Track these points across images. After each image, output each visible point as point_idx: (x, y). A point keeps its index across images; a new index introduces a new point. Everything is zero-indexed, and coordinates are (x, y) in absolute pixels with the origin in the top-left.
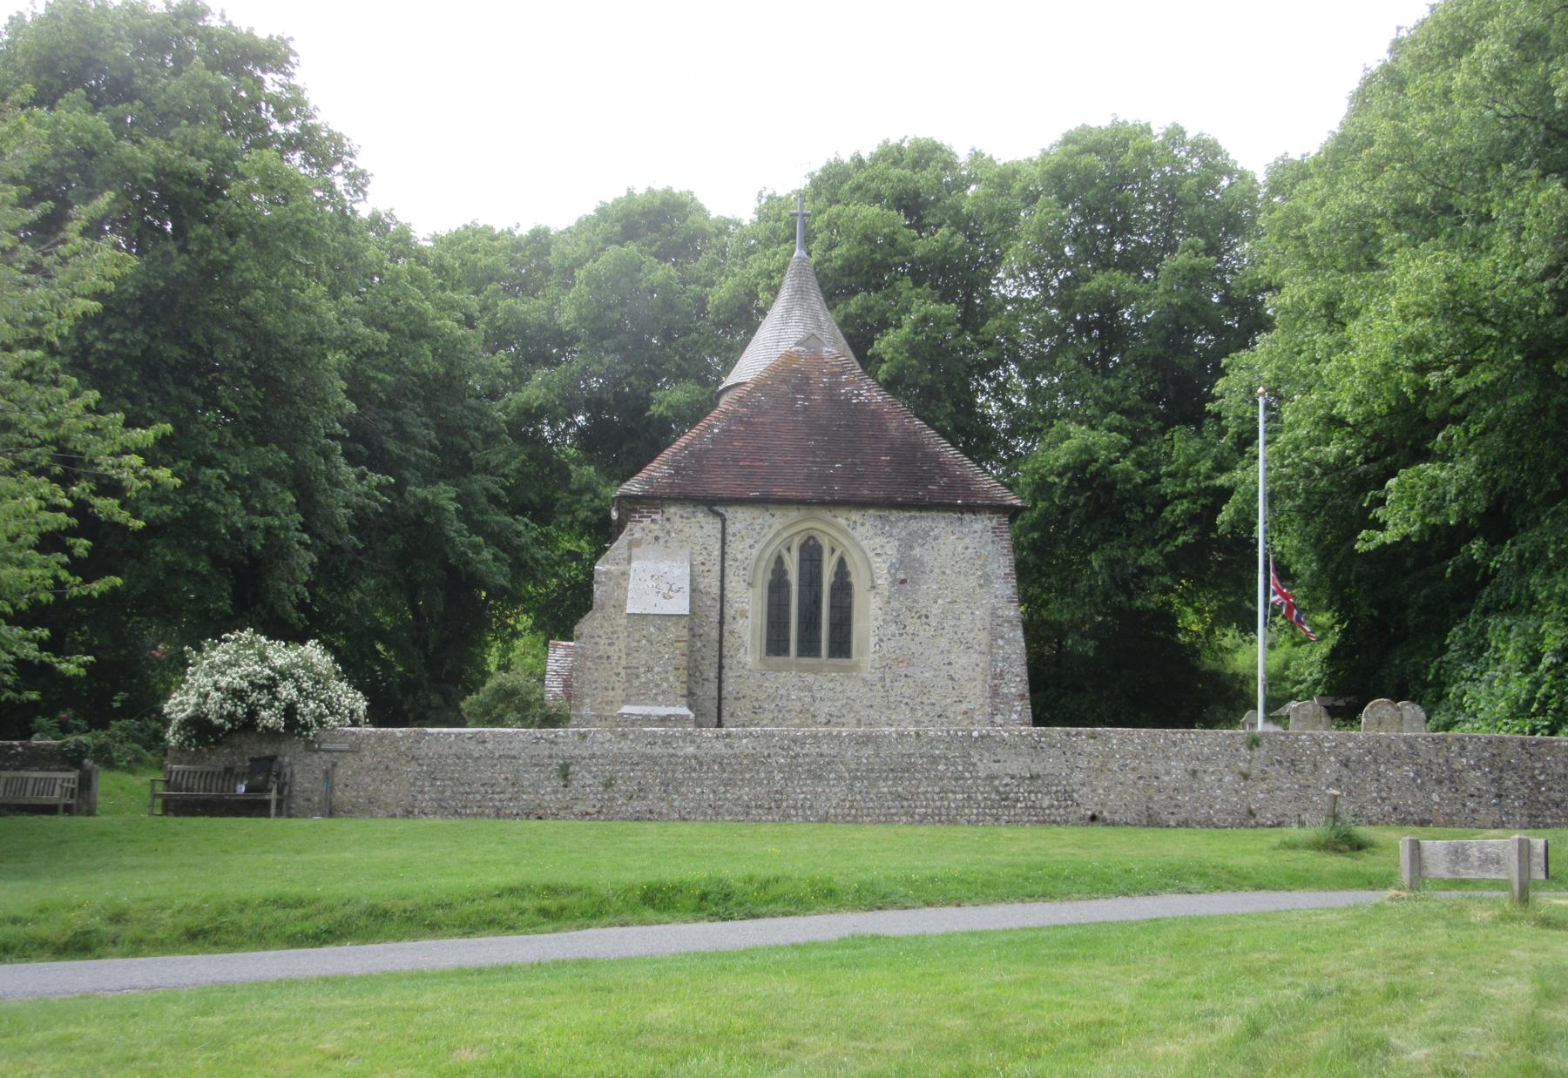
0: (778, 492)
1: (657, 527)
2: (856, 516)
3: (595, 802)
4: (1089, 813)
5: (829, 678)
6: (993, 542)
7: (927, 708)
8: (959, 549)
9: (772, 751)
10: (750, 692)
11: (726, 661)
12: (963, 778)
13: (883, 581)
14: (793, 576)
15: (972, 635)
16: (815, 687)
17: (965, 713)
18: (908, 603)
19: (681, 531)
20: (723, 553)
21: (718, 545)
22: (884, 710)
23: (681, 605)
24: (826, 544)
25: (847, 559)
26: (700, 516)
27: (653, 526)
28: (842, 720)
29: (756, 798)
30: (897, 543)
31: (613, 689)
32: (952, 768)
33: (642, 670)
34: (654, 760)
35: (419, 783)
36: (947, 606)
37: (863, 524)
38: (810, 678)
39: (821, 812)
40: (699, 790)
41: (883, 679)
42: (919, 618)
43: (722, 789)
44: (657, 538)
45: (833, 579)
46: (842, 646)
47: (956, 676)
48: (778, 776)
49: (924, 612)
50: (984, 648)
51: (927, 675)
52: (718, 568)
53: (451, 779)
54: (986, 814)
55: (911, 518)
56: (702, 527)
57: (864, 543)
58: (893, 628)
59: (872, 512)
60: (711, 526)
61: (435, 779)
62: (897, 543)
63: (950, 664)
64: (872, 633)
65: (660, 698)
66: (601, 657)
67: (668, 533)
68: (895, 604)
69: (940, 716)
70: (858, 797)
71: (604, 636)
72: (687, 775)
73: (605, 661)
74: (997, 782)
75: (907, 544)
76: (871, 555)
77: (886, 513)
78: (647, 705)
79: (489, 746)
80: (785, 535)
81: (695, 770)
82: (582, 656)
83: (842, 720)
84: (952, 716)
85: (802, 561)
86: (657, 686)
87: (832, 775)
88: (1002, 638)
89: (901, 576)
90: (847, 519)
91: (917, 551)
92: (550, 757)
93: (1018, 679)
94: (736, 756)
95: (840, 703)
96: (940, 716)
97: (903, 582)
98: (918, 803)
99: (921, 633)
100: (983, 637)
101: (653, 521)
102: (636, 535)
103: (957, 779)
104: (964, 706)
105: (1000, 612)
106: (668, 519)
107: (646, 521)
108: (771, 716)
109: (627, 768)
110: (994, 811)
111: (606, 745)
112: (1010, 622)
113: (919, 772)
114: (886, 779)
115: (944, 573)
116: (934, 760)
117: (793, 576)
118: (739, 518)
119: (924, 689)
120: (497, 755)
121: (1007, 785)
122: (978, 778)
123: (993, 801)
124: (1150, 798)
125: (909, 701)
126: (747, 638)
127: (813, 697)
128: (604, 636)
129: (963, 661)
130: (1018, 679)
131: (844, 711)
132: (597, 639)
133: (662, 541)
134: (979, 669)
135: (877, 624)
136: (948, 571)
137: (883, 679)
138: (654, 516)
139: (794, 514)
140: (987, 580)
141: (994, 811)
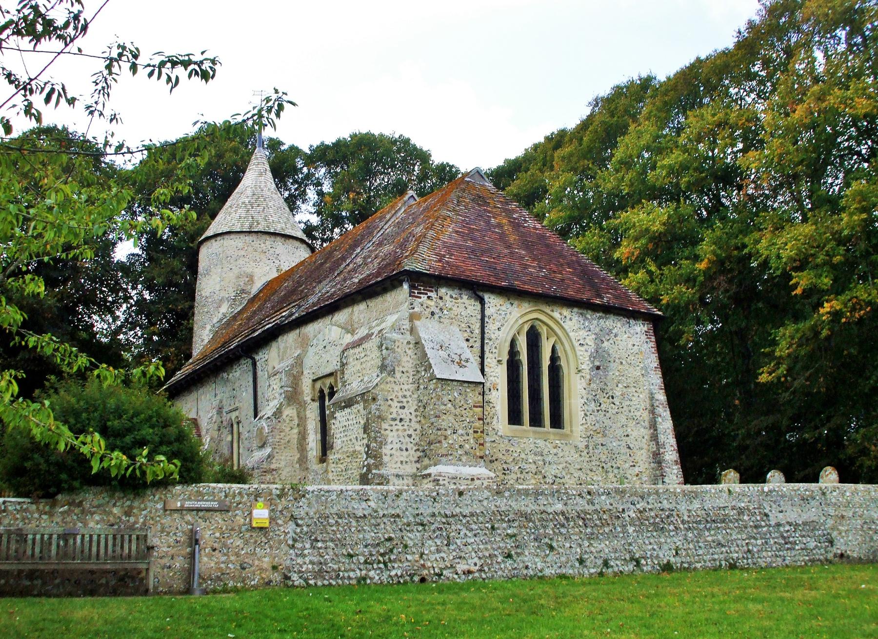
2: (566, 312)
3: (476, 560)
4: (839, 552)
5: (554, 445)
8: (630, 346)
9: (625, 506)
10: (501, 456)
12: (761, 527)
13: (586, 366)
14: (524, 357)
15: (638, 414)
16: (545, 452)
17: (637, 475)
18: (602, 385)
19: (451, 309)
20: (483, 333)
21: (478, 325)
22: (589, 472)
24: (543, 331)
25: (558, 347)
26: (465, 297)
27: (429, 302)
31: (407, 450)
32: (753, 518)
33: (449, 432)
34: (527, 517)
35: (299, 545)
36: (625, 390)
37: (571, 319)
38: (541, 443)
40: (568, 545)
43: (586, 544)
44: (433, 314)
46: (557, 421)
47: (631, 446)
48: (631, 529)
49: (610, 394)
50: (647, 424)
51: (614, 444)
54: (777, 556)
55: (600, 318)
57: (571, 334)
59: (576, 310)
60: (473, 307)
61: (316, 540)
62: (594, 336)
63: (628, 436)
66: (394, 420)
67: (441, 309)
68: (594, 386)
72: (557, 531)
73: (398, 422)
74: (782, 529)
75: (599, 340)
76: (576, 344)
77: (585, 312)
79: (372, 504)
80: (521, 322)
81: (563, 526)
82: (379, 417)
84: (629, 477)
86: (461, 446)
87: (672, 527)
89: (597, 363)
90: (561, 314)
91: (606, 344)
92: (434, 515)
94: (596, 511)
95: (560, 467)
97: (598, 368)
99: (610, 410)
100: (646, 415)
101: (429, 297)
102: (416, 309)
103: (756, 527)
104: (636, 470)
106: (441, 298)
107: (424, 298)
108: (515, 478)
109: (505, 525)
110: (781, 553)
111: (485, 503)
113: (731, 522)
114: (709, 530)
115: (621, 363)
116: (741, 512)
117: (524, 357)
119: (613, 455)
120: (381, 514)
121: (788, 531)
122: (770, 526)
123: (779, 544)
124: (871, 539)
125: (604, 465)
126: (498, 408)
127: (544, 460)
128: (395, 400)
131: (564, 473)
132: (390, 402)
133: (436, 316)
134: (644, 440)
135: (583, 401)
136: (624, 362)
137: (587, 447)
138: (430, 294)
139: (526, 307)
141: (781, 553)
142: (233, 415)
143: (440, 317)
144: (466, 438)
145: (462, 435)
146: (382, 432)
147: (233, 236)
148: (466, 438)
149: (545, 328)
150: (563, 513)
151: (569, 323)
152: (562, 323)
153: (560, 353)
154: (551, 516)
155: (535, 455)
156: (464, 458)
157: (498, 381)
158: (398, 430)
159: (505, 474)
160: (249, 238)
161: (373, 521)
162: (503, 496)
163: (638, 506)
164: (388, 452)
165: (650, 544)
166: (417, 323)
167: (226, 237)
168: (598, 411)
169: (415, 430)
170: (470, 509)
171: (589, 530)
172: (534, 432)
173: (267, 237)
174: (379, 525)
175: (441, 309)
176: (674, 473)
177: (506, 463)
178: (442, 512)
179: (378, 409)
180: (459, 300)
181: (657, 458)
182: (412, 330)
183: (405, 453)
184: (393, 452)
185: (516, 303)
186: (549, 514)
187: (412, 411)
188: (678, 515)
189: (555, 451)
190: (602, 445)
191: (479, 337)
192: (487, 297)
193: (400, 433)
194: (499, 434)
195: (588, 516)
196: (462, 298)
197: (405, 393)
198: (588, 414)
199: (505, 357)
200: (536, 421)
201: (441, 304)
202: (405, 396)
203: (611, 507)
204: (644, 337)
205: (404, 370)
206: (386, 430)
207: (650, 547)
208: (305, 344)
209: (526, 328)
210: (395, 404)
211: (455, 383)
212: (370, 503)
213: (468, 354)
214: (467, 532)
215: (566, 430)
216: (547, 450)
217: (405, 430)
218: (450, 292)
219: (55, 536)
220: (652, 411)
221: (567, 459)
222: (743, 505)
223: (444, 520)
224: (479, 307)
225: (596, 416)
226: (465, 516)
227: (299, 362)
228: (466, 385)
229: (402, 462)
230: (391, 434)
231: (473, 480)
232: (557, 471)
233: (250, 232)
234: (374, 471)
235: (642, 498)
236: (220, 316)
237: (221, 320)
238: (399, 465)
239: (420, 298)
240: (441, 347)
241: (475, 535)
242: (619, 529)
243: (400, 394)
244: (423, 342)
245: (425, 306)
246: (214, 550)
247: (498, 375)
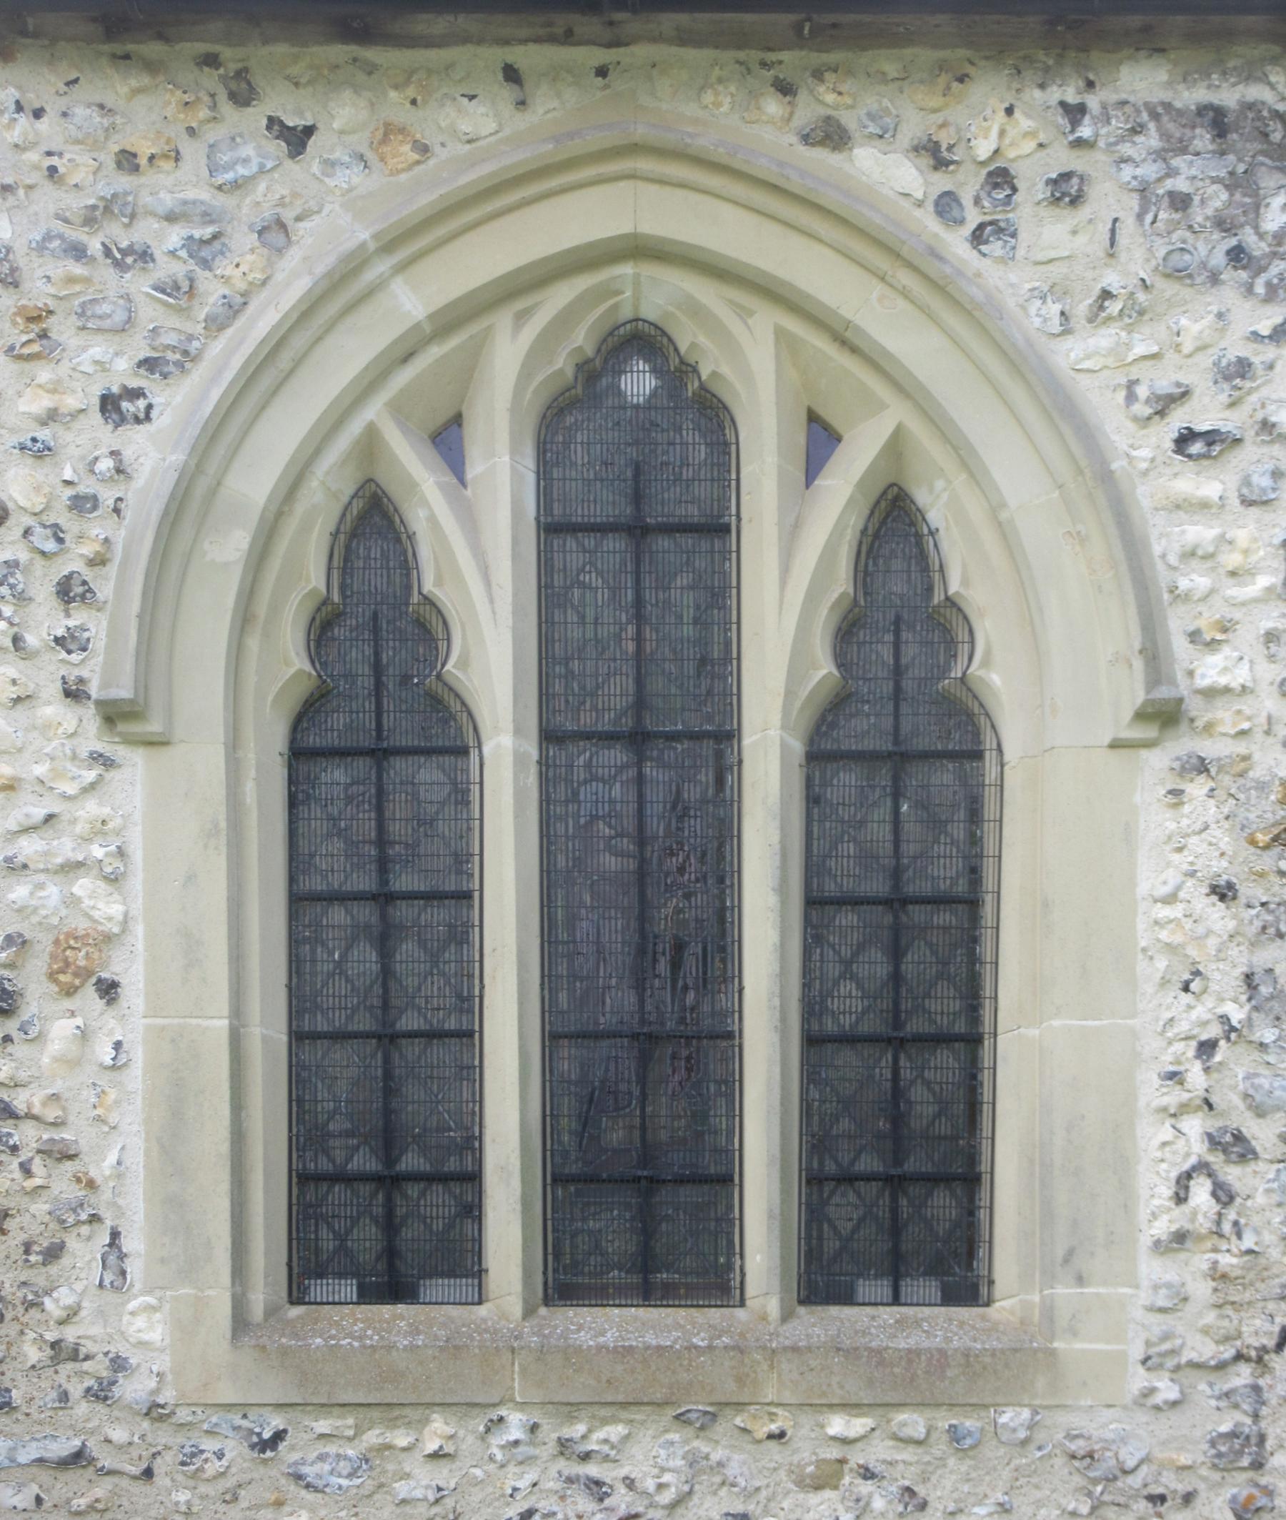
45: (824, 668)
64: (1152, 1093)
152: (956, 243)
157: (108, 909)
194: (134, 1389)
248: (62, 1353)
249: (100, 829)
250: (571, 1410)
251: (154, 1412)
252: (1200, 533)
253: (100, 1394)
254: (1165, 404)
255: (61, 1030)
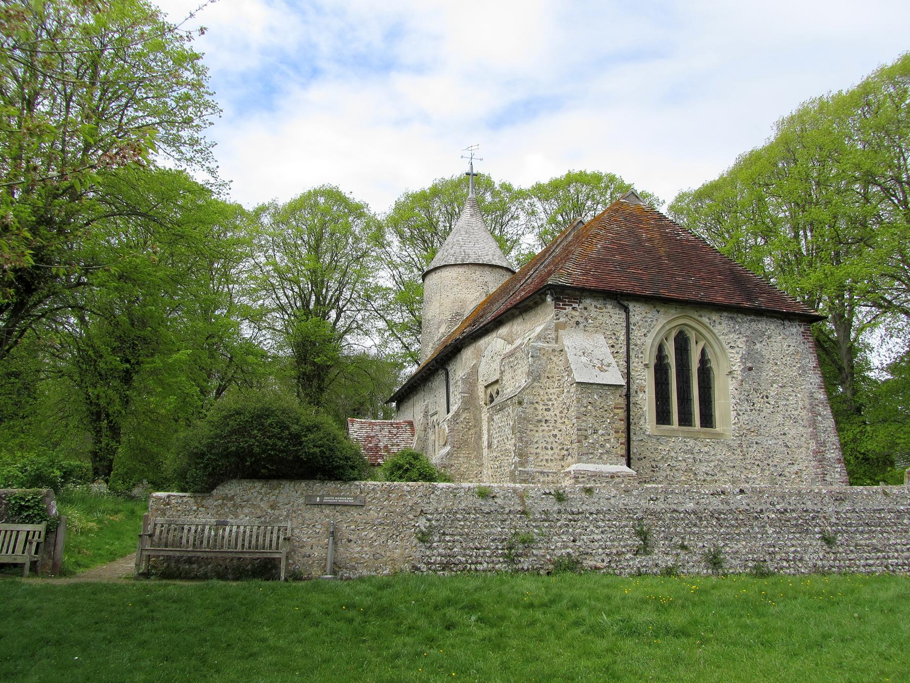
0: (664, 293)
1: (577, 314)
2: (715, 317)
6: (804, 343)
7: (772, 469)
9: (764, 507)
10: (649, 454)
11: (622, 425)
13: (737, 368)
14: (672, 361)
15: (796, 413)
19: (596, 318)
20: (628, 339)
21: (624, 332)
22: (743, 470)
23: (615, 377)
24: (692, 336)
26: (610, 307)
27: (574, 313)
28: (715, 478)
29: (751, 552)
30: (745, 339)
31: (552, 449)
33: (590, 432)
36: (780, 390)
37: (720, 323)
38: (691, 443)
39: (810, 564)
40: (701, 544)
41: (740, 445)
42: (762, 398)
46: (707, 420)
47: (789, 444)
49: (765, 393)
51: (770, 443)
52: (624, 349)
53: (461, 535)
55: (752, 321)
56: (612, 316)
57: (720, 338)
58: (746, 406)
59: (725, 314)
61: (444, 534)
62: (745, 339)
63: (784, 434)
65: (605, 457)
66: (540, 421)
67: (586, 319)
69: (780, 475)
70: (841, 550)
71: (541, 403)
75: (751, 342)
77: (735, 316)
78: (595, 463)
79: (499, 501)
80: (668, 328)
81: (695, 525)
83: (715, 478)
84: (788, 475)
85: (676, 349)
86: (602, 446)
87: (817, 529)
88: (820, 415)
91: (758, 346)
92: (559, 512)
93: (835, 447)
94: (731, 511)
95: (712, 464)
96: (780, 475)
97: (750, 369)
98: (891, 554)
101: (573, 308)
102: (561, 320)
104: (795, 468)
105: (815, 396)
106: (586, 309)
107: (569, 309)
108: (665, 475)
111: (612, 501)
112: (822, 403)
115: (776, 364)
117: (672, 361)
118: (638, 312)
119: (769, 454)
120: (507, 510)
128: (541, 403)
129: (793, 432)
130: (835, 447)
133: (581, 326)
137: (740, 445)
139: (673, 313)
140: (803, 371)
142: (435, 418)
143: (585, 326)
144: (606, 437)
145: (603, 435)
146: (528, 432)
147: (448, 269)
148: (606, 437)
149: (693, 333)
150: (694, 513)
151: (719, 327)
152: (711, 327)
153: (710, 355)
154: (682, 515)
155: (685, 453)
156: (605, 457)
158: (543, 431)
159: (654, 471)
160: (461, 270)
161: (500, 517)
162: (631, 495)
163: (778, 507)
164: (533, 451)
165: (793, 546)
166: (561, 332)
167: (443, 270)
168: (751, 410)
169: (560, 431)
170: (597, 507)
171: (723, 530)
172: (683, 431)
173: (477, 268)
174: (505, 520)
175: (586, 319)
176: (838, 473)
177: (654, 460)
178: (569, 509)
179: (524, 412)
180: (604, 310)
181: (819, 456)
182: (557, 340)
183: (550, 452)
184: (539, 451)
185: (662, 310)
186: (680, 513)
187: (557, 412)
188: (824, 517)
189: (706, 449)
190: (757, 443)
191: (625, 343)
192: (631, 306)
193: (546, 434)
195: (722, 516)
196: (606, 308)
197: (550, 397)
198: (741, 413)
199: (653, 362)
200: (685, 419)
201: (586, 314)
202: (550, 400)
203: (748, 508)
204: (800, 338)
205: (550, 375)
206: (531, 430)
207: (793, 549)
208: (479, 355)
209: (674, 334)
210: (540, 407)
211: (595, 387)
212: (496, 500)
213: (610, 359)
214: (594, 529)
215: (719, 428)
216: (697, 448)
217: (550, 431)
218: (594, 303)
219: (207, 527)
220: (812, 410)
221: (719, 457)
222: (902, 508)
223: (570, 517)
224: (624, 316)
225: (749, 415)
226: (591, 514)
227: (475, 370)
228: (607, 388)
229: (547, 460)
230: (537, 435)
231: (612, 477)
232: (708, 469)
233: (462, 265)
234: (519, 469)
235: (783, 498)
236: (440, 335)
237: (441, 338)
238: (544, 463)
239: (565, 309)
240: (584, 353)
241: (602, 532)
242: (757, 530)
243: (546, 397)
244: (566, 349)
245: (570, 316)
246: (350, 541)
247: (645, 379)
248: (641, 429)
249: (644, 376)
250: (685, 437)
251: (649, 436)
252: (732, 355)
253: (644, 433)
254: (729, 343)
255: (641, 395)
